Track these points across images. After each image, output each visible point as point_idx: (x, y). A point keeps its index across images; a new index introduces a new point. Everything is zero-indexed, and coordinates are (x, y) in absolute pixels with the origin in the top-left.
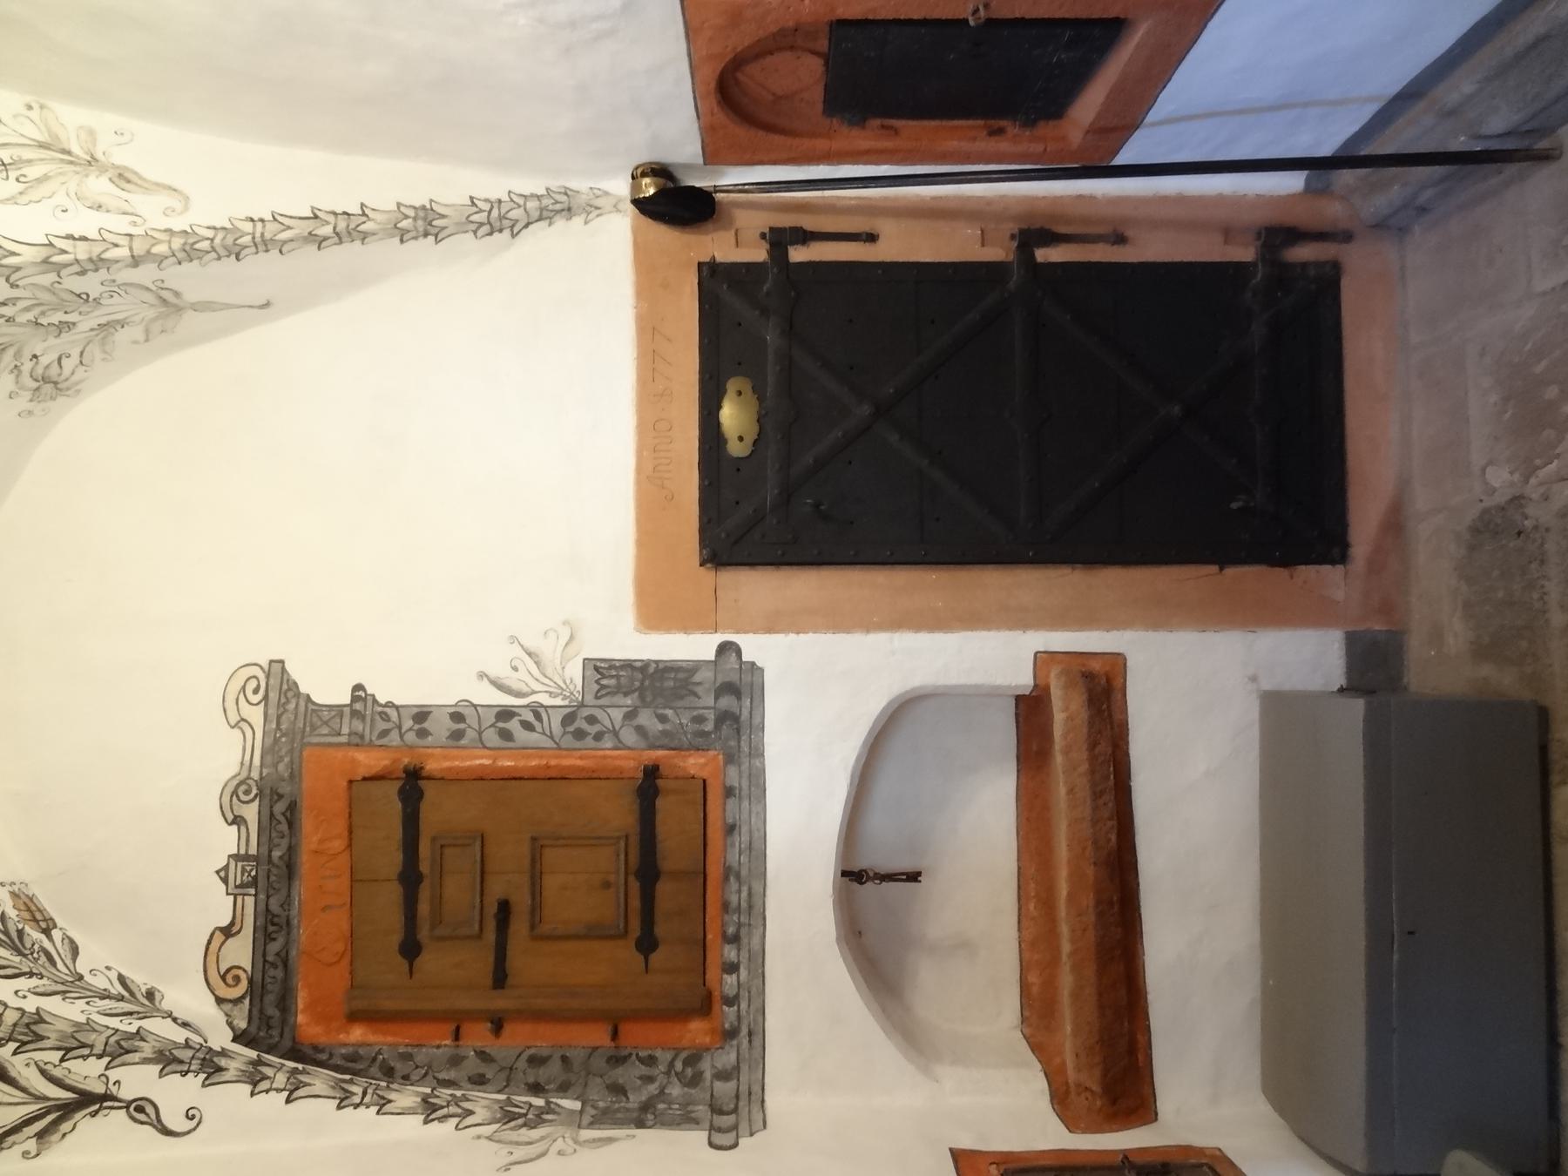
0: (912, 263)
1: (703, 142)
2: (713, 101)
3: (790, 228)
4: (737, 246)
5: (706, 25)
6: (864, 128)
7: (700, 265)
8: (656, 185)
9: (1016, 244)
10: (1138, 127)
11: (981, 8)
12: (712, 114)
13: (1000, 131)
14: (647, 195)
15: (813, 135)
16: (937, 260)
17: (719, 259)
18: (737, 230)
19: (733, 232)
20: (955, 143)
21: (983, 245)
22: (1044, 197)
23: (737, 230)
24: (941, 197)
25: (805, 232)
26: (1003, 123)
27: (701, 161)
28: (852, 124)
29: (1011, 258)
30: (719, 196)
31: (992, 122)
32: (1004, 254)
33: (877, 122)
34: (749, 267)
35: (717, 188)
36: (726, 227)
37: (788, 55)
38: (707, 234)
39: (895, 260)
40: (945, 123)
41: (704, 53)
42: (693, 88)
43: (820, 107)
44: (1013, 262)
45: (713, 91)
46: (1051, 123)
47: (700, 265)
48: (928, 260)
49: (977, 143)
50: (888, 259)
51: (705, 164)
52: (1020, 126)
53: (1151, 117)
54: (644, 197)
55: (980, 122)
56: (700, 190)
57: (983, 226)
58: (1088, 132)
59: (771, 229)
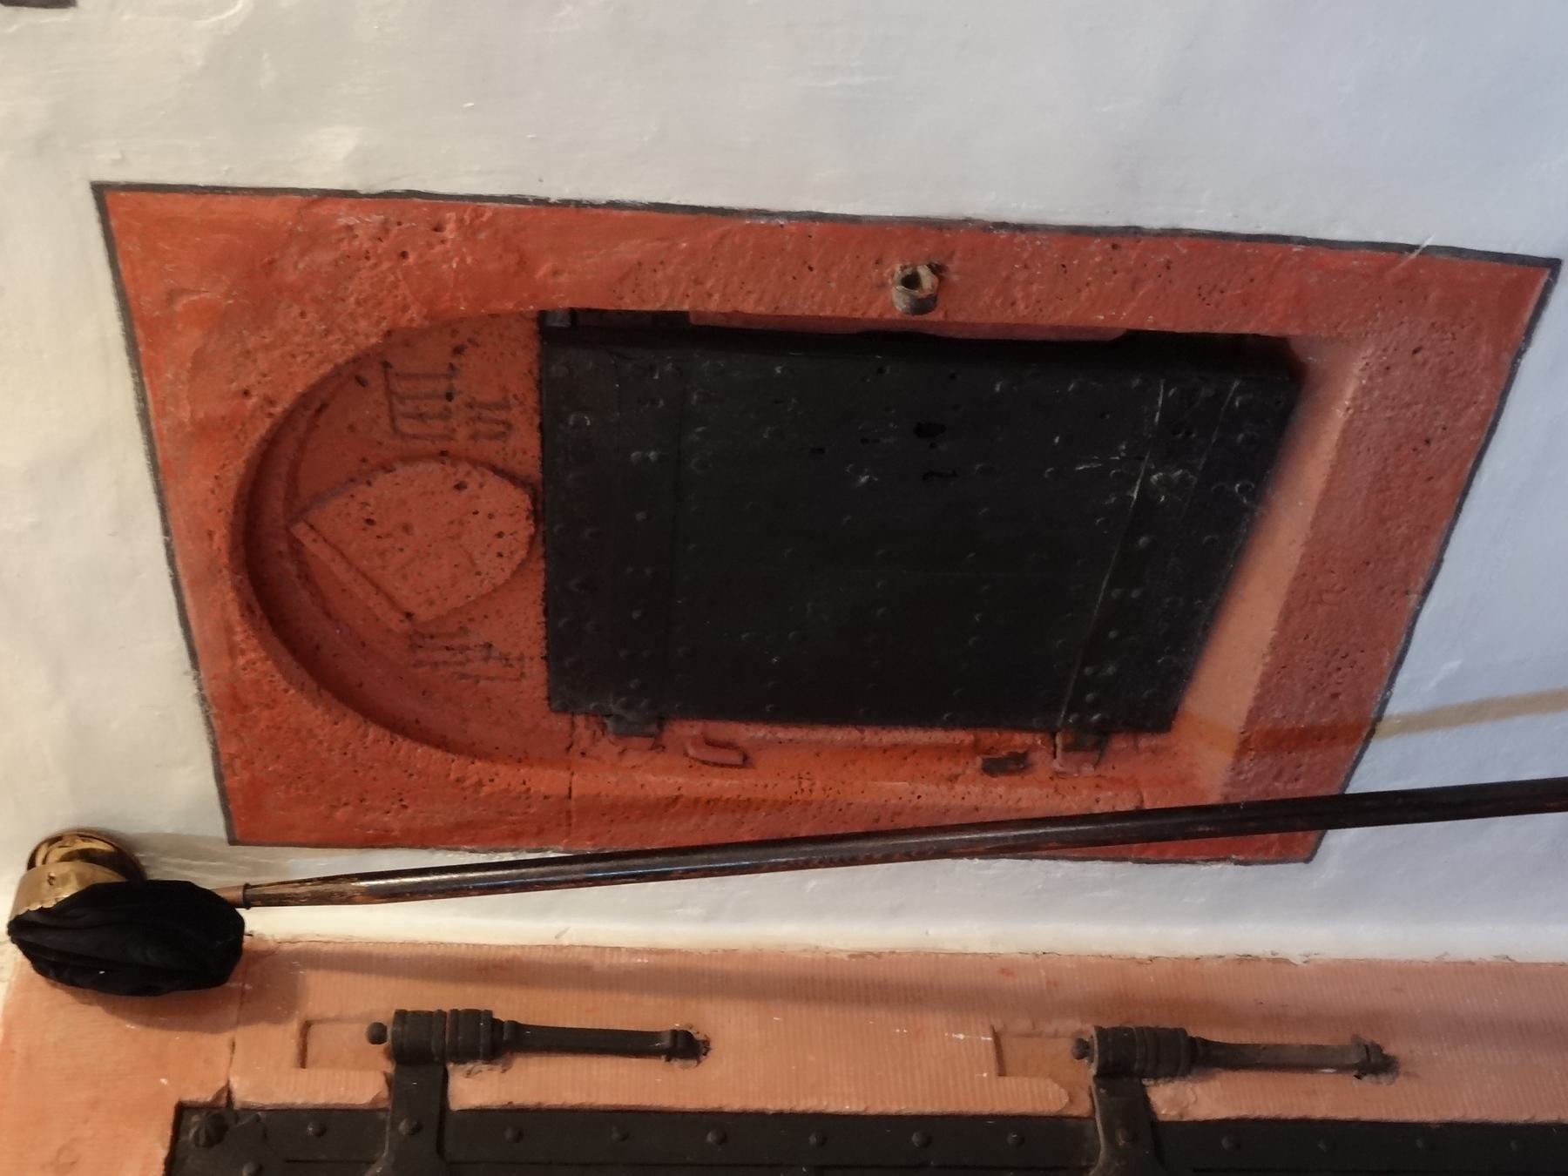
0: (804, 1116)
1: (216, 755)
2: (226, 597)
3: (455, 1012)
4: (303, 1061)
5: (179, 307)
6: (658, 747)
7: (182, 1110)
8: (80, 877)
9: (1093, 1071)
10: (1372, 733)
11: (924, 272)
12: (233, 651)
13: (1016, 764)
14: (50, 904)
15: (521, 760)
16: (877, 1108)
17: (246, 1092)
18: (307, 1026)
19: (294, 1026)
20: (901, 785)
21: (1002, 1072)
22: (1151, 959)
23: (307, 1026)
24: (878, 955)
25: (496, 1025)
26: (1020, 740)
27: (215, 826)
28: (625, 732)
29: (1082, 1108)
30: (262, 924)
31: (990, 737)
32: (1066, 1100)
33: (687, 731)
34: (328, 1119)
35: (249, 892)
36: (277, 1019)
37: (432, 472)
38: (216, 1029)
39: (754, 1104)
40: (871, 736)
41: (185, 414)
42: (168, 546)
43: (537, 673)
44: (1091, 1118)
45: (224, 560)
46: (1144, 742)
47: (182, 1110)
48: (848, 1107)
49: (959, 788)
50: (734, 1103)
51: (233, 841)
52: (1066, 749)
53: (1395, 708)
54: (41, 910)
55: (963, 737)
56: (209, 896)
57: (998, 1027)
58: (1244, 747)
59: (401, 1015)
